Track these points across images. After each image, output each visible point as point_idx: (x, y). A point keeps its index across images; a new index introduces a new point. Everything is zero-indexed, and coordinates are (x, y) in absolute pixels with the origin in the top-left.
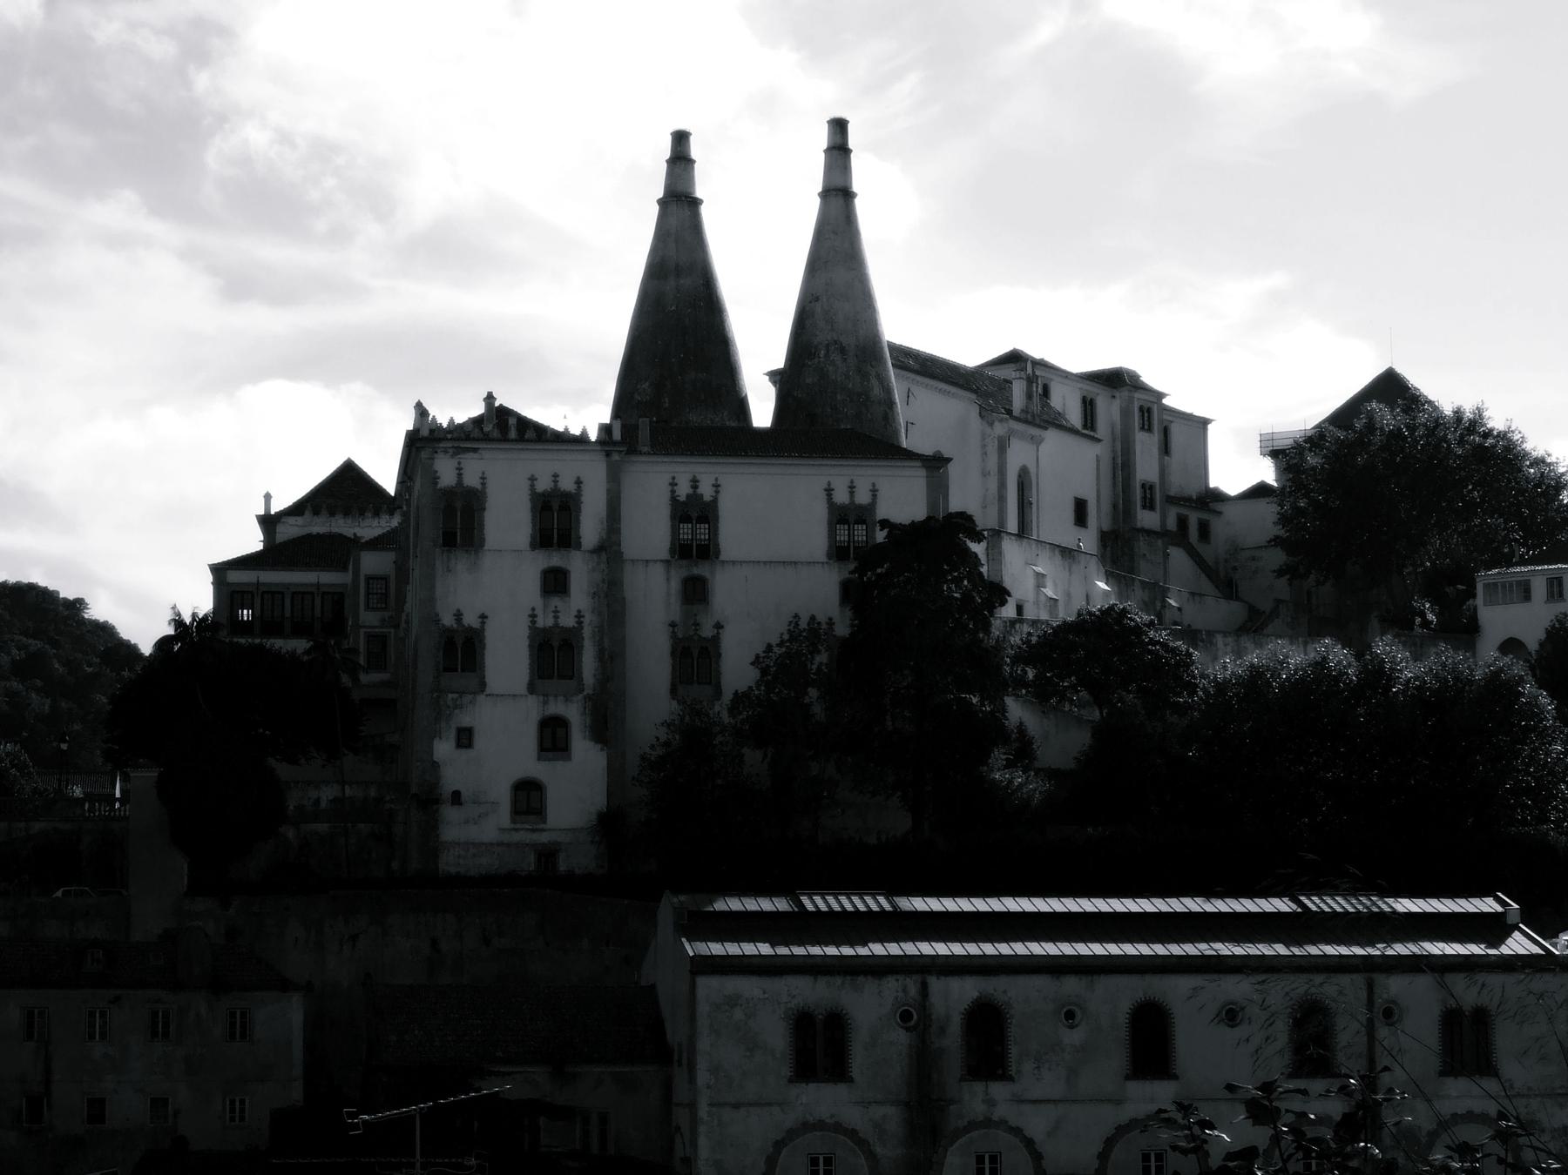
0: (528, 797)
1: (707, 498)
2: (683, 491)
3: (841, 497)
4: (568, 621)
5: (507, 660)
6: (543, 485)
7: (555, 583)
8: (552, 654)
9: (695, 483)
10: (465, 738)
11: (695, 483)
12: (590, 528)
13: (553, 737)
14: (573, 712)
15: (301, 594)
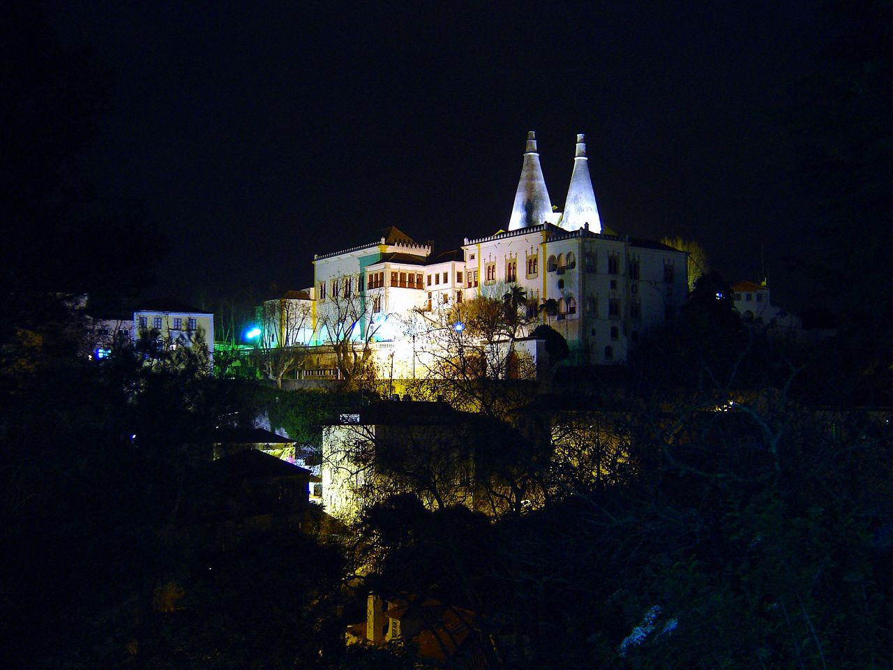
0: (609, 351)
1: (637, 260)
2: (631, 258)
3: (666, 263)
4: (617, 297)
5: (603, 309)
6: (611, 254)
7: (613, 285)
8: (614, 309)
9: (634, 255)
10: (594, 333)
11: (634, 255)
12: (622, 267)
13: (614, 334)
14: (620, 328)
15: (411, 276)
